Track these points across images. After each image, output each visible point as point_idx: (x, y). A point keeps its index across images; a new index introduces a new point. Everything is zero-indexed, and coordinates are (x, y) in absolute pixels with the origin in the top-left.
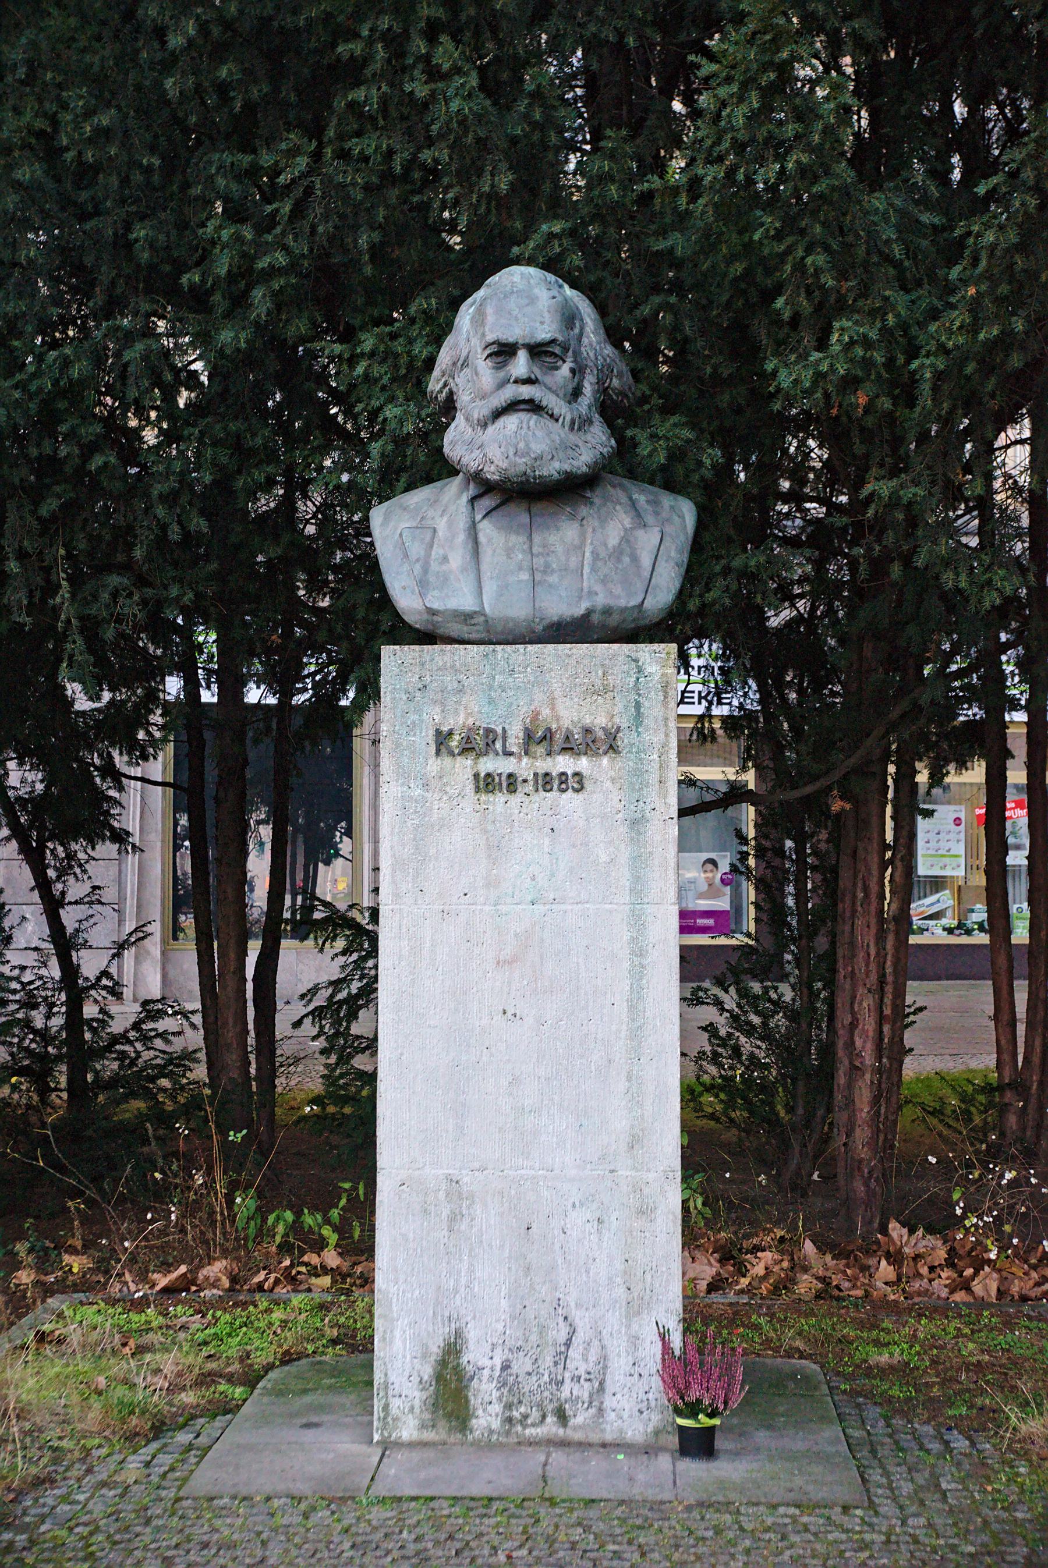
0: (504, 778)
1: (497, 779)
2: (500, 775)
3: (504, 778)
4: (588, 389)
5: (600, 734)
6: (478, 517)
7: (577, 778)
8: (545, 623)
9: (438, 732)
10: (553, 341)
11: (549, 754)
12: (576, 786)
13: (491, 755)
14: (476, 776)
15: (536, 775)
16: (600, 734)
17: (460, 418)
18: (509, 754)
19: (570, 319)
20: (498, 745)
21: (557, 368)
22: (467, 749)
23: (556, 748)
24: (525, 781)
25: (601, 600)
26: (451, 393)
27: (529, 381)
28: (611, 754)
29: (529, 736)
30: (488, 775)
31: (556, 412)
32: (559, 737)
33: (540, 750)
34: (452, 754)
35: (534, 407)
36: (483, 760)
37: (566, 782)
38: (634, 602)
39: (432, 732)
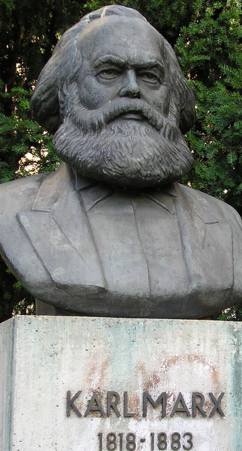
0: (124, 438)
1: (118, 438)
2: (121, 435)
3: (124, 438)
4: (174, 109)
5: (207, 398)
6: (88, 207)
7: (187, 438)
8: (158, 301)
9: (69, 393)
10: (157, 66)
11: (163, 415)
12: (187, 445)
13: (114, 415)
14: (100, 435)
15: (152, 435)
16: (207, 398)
17: (67, 122)
18: (128, 416)
19: (163, 52)
20: (120, 407)
21: (156, 88)
22: (94, 408)
23: (169, 411)
24: (143, 441)
25: (204, 282)
26: (57, 101)
27: (138, 96)
28: (217, 417)
29: (147, 398)
30: (112, 434)
31: (159, 122)
32: (171, 401)
33: (157, 412)
34: (79, 415)
35: (142, 117)
36: (108, 421)
37: (178, 442)
38: (227, 285)
39: (65, 395)
